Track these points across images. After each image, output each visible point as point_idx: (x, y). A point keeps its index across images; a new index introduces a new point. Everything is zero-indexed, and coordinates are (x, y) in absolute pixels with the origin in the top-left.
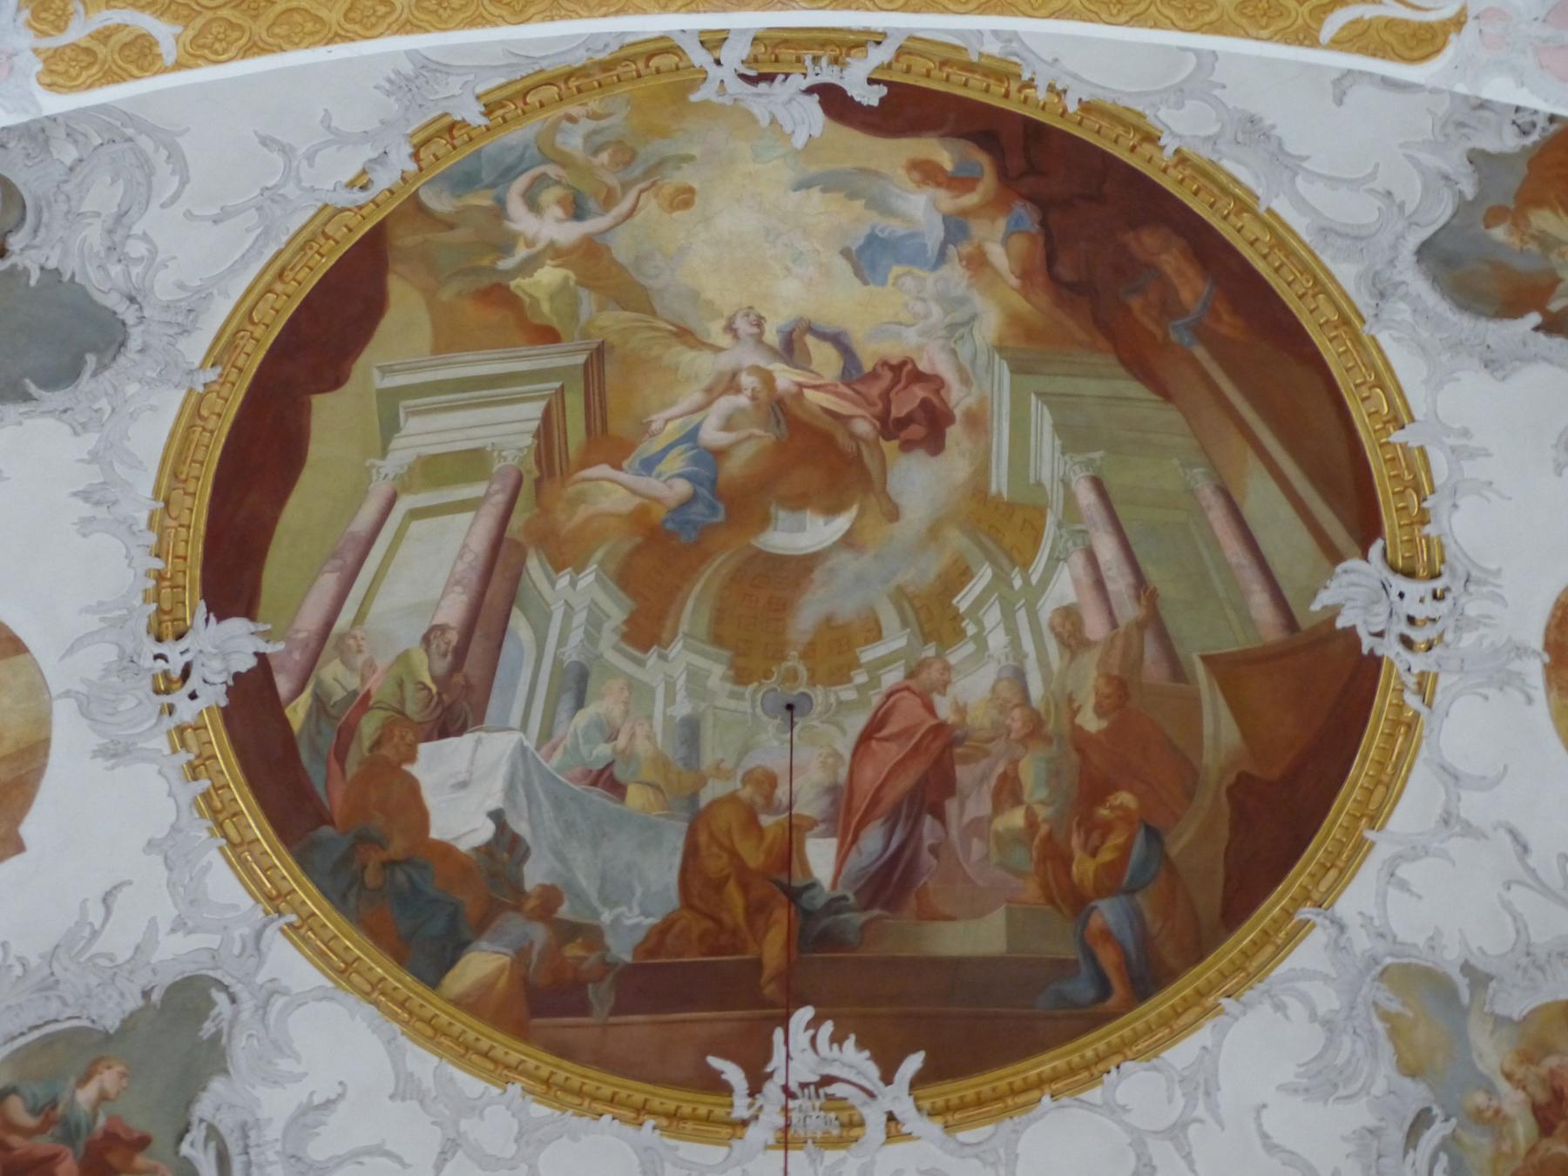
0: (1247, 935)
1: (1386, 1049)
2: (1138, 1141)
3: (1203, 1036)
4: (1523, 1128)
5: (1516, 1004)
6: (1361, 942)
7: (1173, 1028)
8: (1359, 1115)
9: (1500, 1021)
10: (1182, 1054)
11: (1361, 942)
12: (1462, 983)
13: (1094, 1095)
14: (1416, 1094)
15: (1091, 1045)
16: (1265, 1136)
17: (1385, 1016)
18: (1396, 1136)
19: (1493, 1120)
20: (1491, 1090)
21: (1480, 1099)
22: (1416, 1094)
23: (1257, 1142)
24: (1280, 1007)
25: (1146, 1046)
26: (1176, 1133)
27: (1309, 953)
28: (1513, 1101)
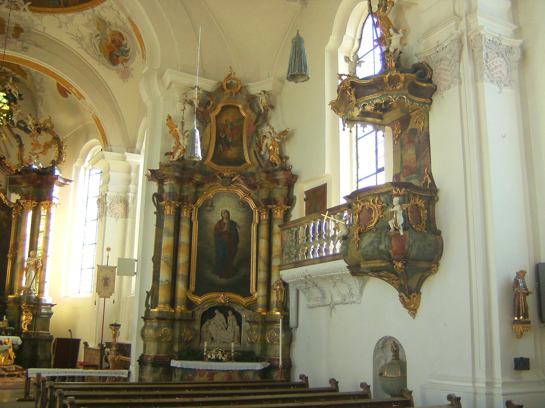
0: (81, 6)
1: (96, 26)
2: (61, 22)
3: (73, 14)
4: (110, 42)
5: (113, 29)
6: (96, 13)
7: (69, 12)
8: (91, 31)
9: (111, 30)
10: (69, 15)
11: (96, 13)
12: (108, 23)
13: (56, 15)
14: (98, 32)
15: (56, 10)
16: (78, 28)
17: (97, 22)
18: (94, 36)
19: (107, 40)
20: (107, 36)
21: (106, 36)
22: (98, 32)
23: (77, 29)
24: (84, 15)
25: (65, 12)
26: (66, 24)
27: (90, 11)
28: (109, 38)
